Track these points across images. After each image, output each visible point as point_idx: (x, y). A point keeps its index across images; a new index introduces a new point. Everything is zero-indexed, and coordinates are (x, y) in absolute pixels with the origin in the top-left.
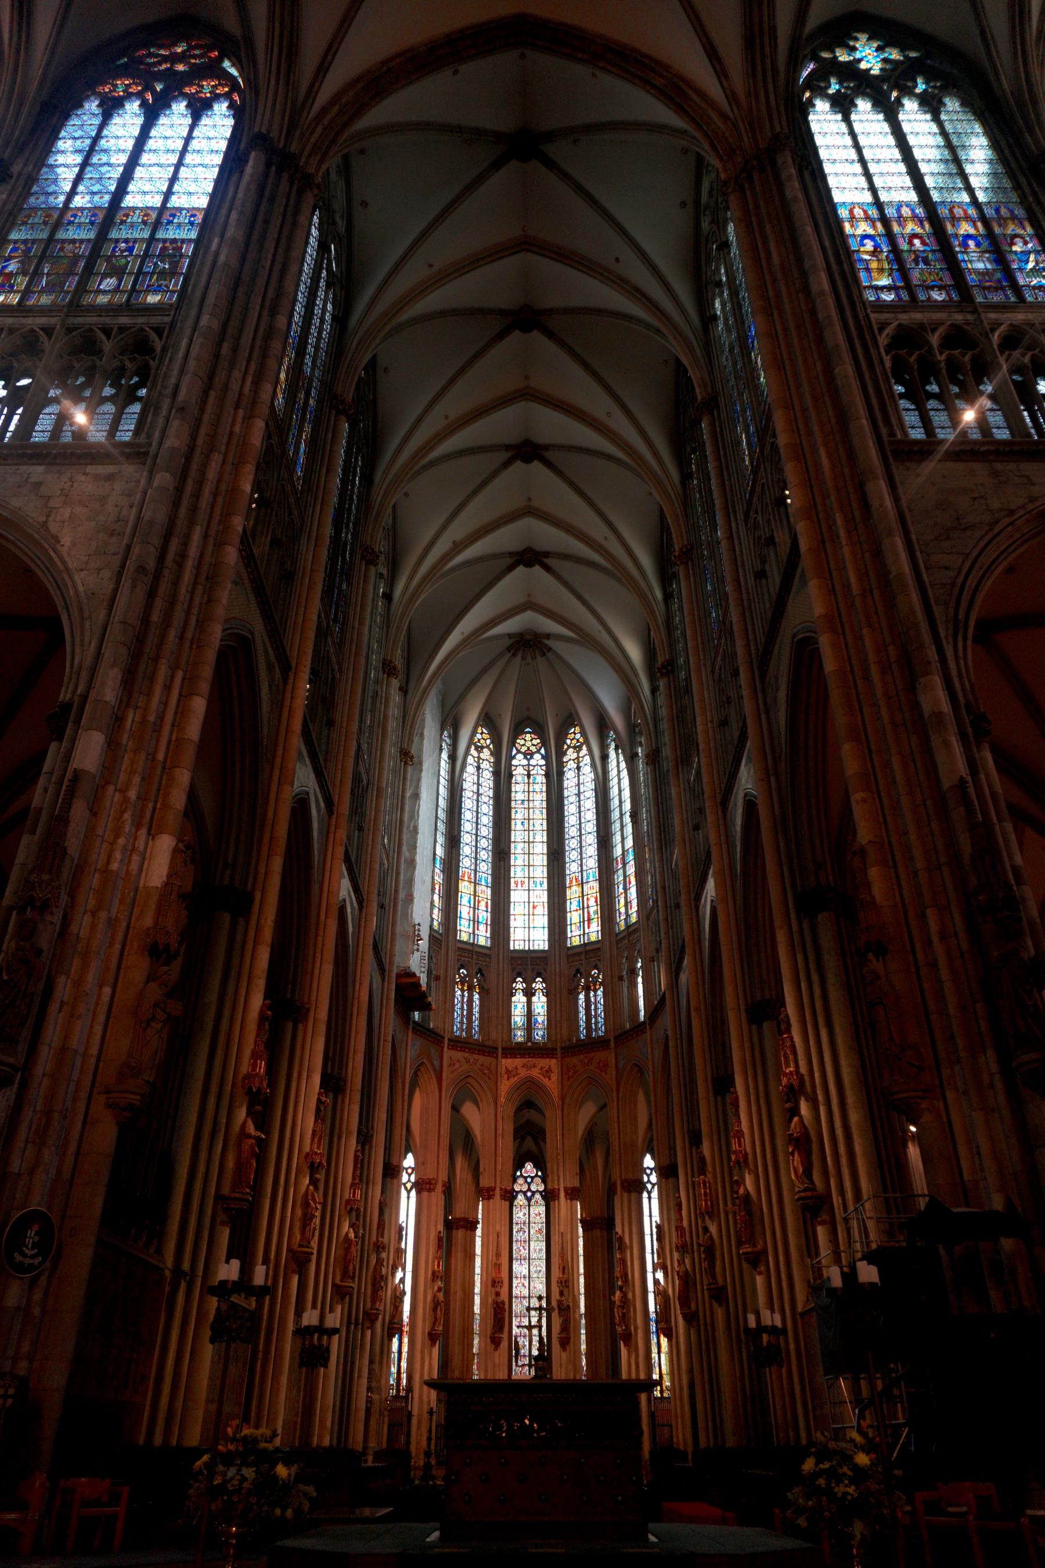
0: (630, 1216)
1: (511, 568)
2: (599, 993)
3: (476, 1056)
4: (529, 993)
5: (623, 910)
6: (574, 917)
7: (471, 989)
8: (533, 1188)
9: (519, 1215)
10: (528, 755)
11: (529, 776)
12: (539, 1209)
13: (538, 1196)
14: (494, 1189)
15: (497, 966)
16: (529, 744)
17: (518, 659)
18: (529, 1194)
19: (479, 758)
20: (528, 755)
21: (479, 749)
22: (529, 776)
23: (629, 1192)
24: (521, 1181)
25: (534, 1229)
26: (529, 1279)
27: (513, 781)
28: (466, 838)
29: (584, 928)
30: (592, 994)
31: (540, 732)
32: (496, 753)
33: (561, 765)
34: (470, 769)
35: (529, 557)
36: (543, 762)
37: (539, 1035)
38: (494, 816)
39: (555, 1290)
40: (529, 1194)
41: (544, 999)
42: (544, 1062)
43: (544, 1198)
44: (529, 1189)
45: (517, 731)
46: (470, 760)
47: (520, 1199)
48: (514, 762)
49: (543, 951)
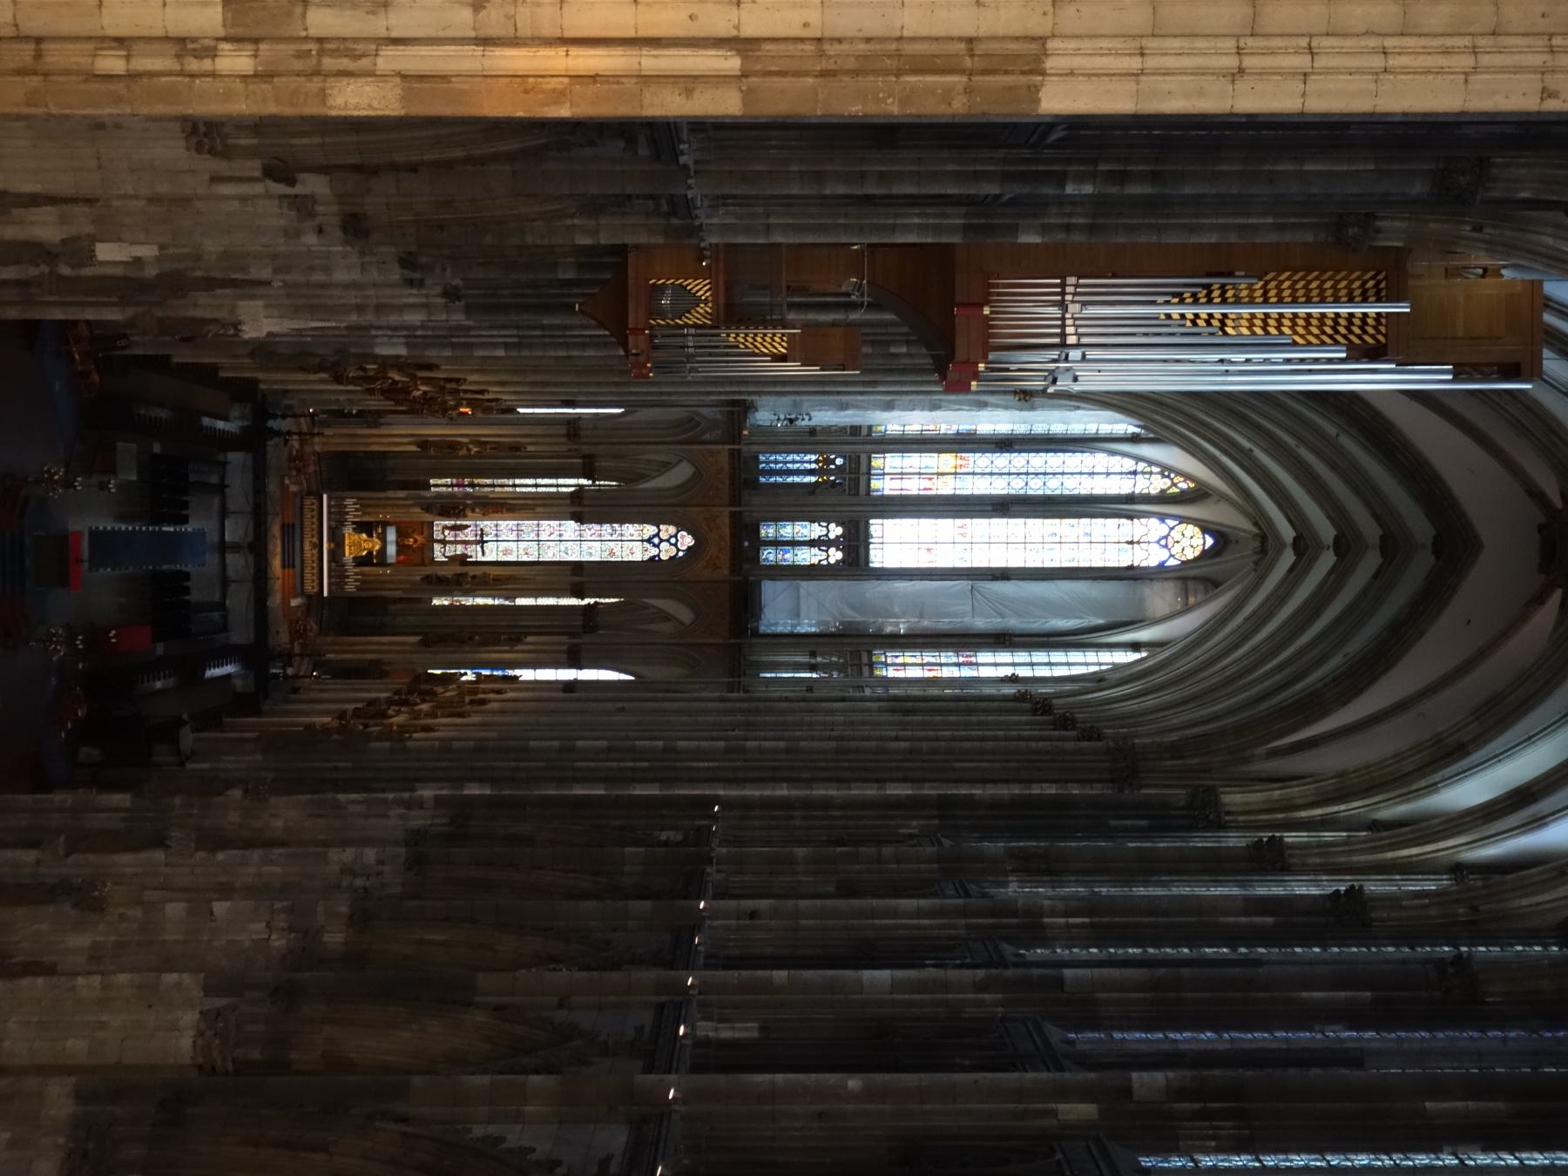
0: (545, 652)
3: (727, 481)
5: (900, 660)
11: (1131, 543)
13: (654, 551)
14: (581, 505)
15: (851, 502)
16: (1185, 542)
18: (656, 540)
19: (1151, 473)
22: (1131, 543)
25: (616, 547)
26: (508, 541)
27: (1123, 521)
32: (1163, 498)
36: (1153, 563)
38: (1061, 496)
39: (478, 571)
40: (656, 540)
41: (815, 561)
42: (725, 559)
43: (652, 559)
44: (661, 541)
48: (1154, 522)
49: (867, 561)
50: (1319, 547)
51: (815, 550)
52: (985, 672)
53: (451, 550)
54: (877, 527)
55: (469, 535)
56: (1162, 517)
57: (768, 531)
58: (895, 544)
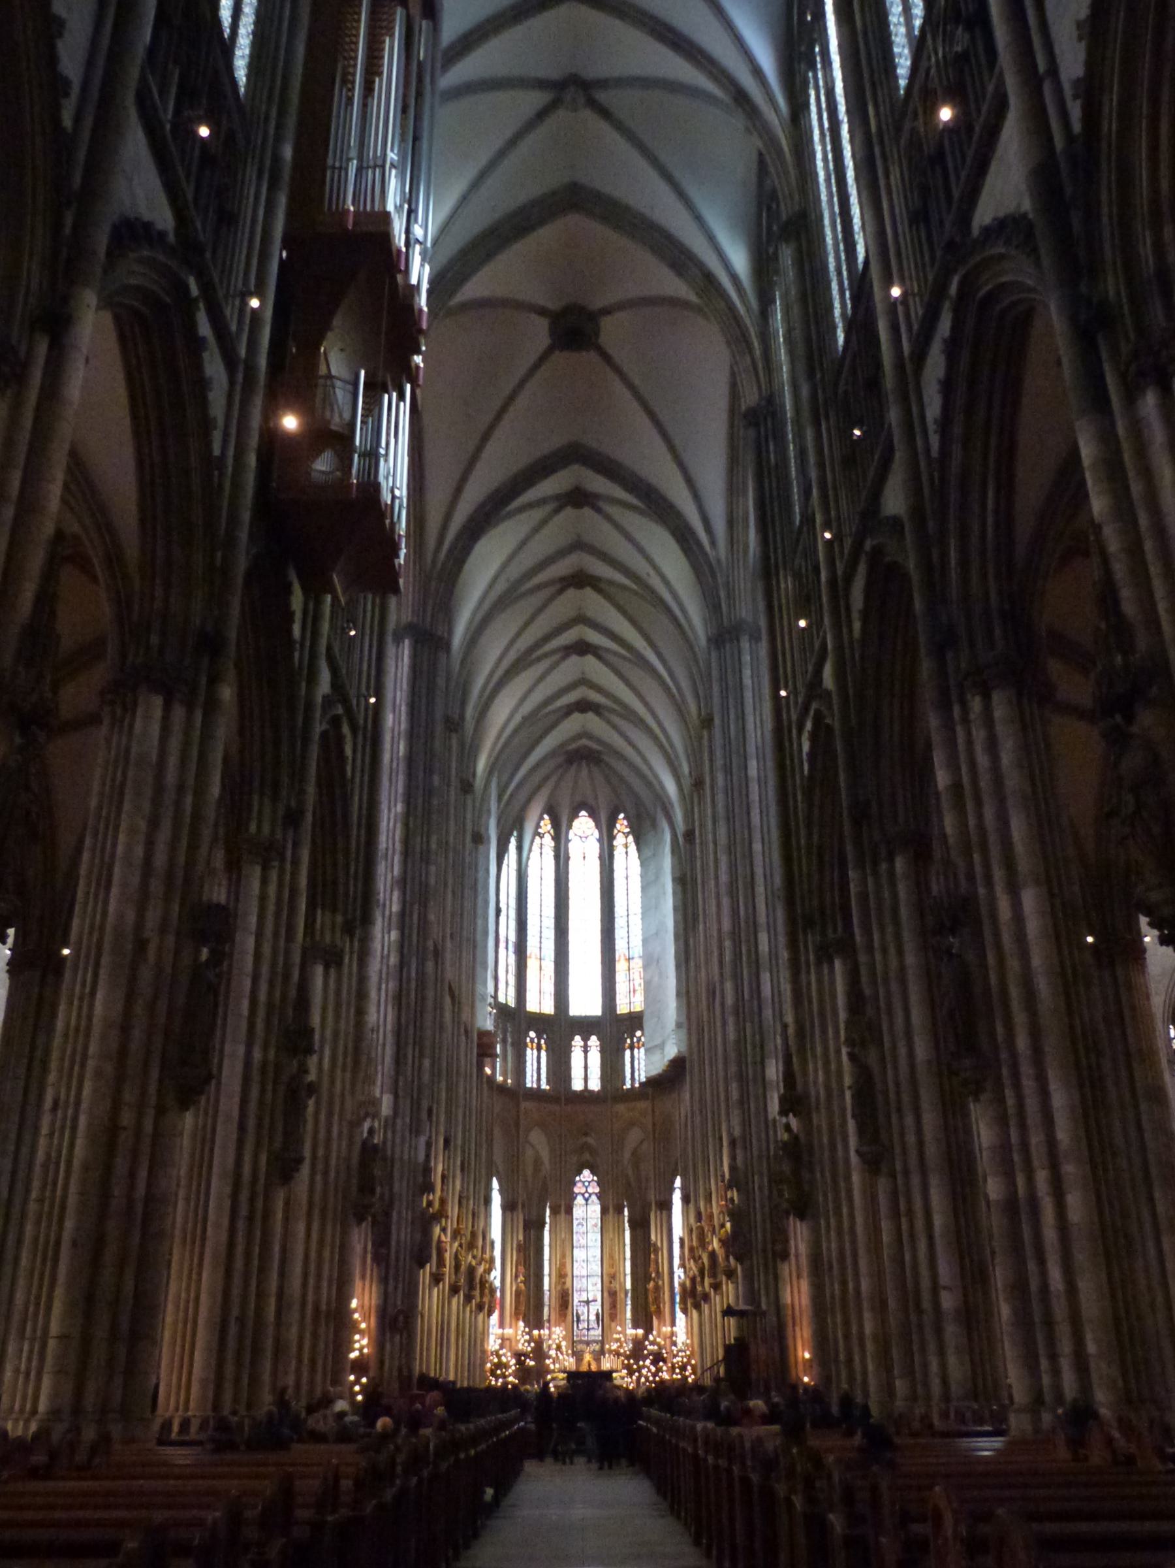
2: (642, 1050)
4: (586, 1051)
7: (539, 1048)
8: (590, 1190)
9: (578, 1212)
12: (595, 1208)
13: (594, 1197)
15: (559, 1029)
21: (541, 836)
23: (661, 1211)
24: (579, 1185)
30: (636, 1051)
31: (593, 815)
32: (557, 838)
33: (611, 849)
34: (535, 854)
35: (583, 706)
36: (598, 845)
37: (595, 1085)
40: (587, 1195)
45: (574, 815)
47: (579, 1200)
48: (570, 845)
50: (584, 681)
51: (589, 1054)
53: (593, 1324)
55: (582, 1310)
56: (568, 841)
57: (577, 1085)
58: (585, 1002)
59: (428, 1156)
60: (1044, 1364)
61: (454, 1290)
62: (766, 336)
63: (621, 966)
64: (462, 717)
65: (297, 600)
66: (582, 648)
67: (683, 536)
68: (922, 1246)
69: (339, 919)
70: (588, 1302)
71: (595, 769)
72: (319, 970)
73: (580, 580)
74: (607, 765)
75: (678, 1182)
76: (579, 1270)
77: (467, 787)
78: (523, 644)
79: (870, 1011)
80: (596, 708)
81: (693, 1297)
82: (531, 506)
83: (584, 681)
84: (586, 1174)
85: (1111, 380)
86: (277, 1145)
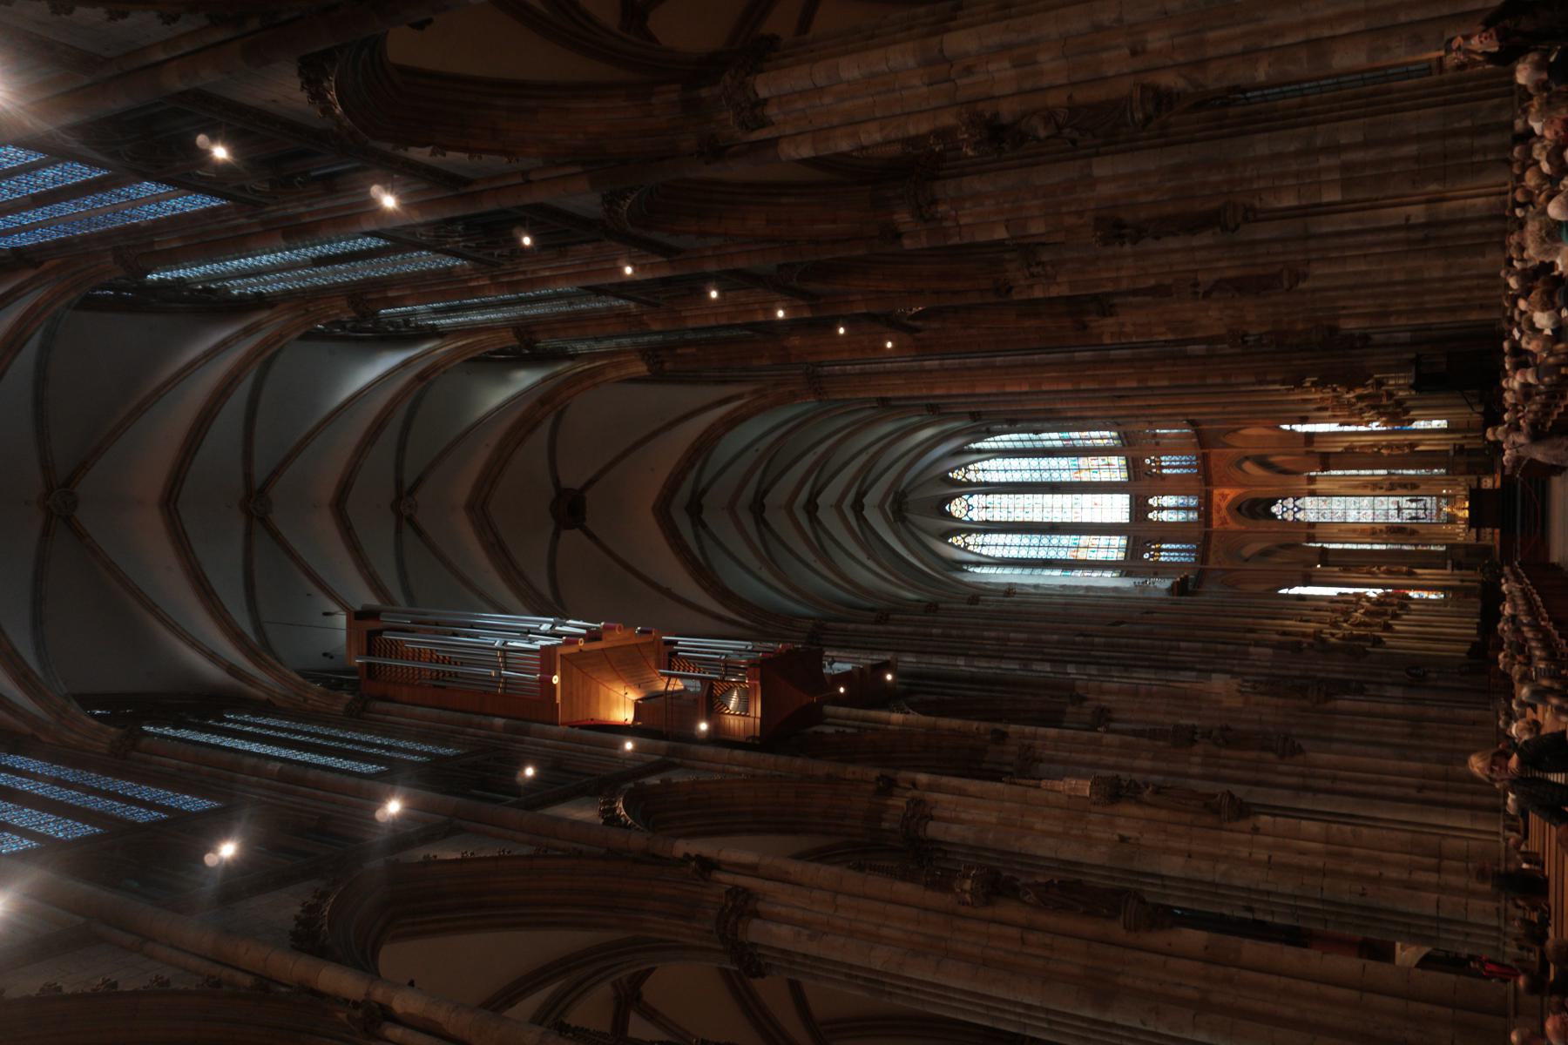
1: (865, 520)
4: (1161, 509)
6: (1105, 476)
9: (1312, 517)
10: (969, 508)
12: (1309, 502)
15: (1140, 532)
17: (910, 516)
20: (969, 508)
28: (1042, 554)
29: (1114, 469)
31: (949, 499)
32: (969, 532)
33: (979, 484)
34: (985, 551)
35: (858, 507)
45: (949, 515)
46: (977, 550)
50: (838, 506)
52: (1055, 435)
53: (1421, 505)
54: (1123, 517)
55: (1406, 514)
58: (1116, 508)
59: (1267, 646)
60: (1478, 158)
61: (1387, 627)
62: (593, 356)
63: (1085, 477)
64: (872, 610)
65: (830, 730)
66: (811, 507)
67: (731, 422)
68: (1369, 238)
69: (1070, 709)
70: (1399, 509)
71: (910, 498)
72: (1113, 725)
73: (758, 508)
74: (909, 484)
75: (1286, 427)
76: (1367, 517)
77: (932, 608)
78: (810, 557)
79: (1168, 281)
80: (861, 495)
81: (1397, 413)
82: (701, 548)
83: (838, 506)
84: (1274, 509)
85: (756, 136)
86: (1271, 756)
